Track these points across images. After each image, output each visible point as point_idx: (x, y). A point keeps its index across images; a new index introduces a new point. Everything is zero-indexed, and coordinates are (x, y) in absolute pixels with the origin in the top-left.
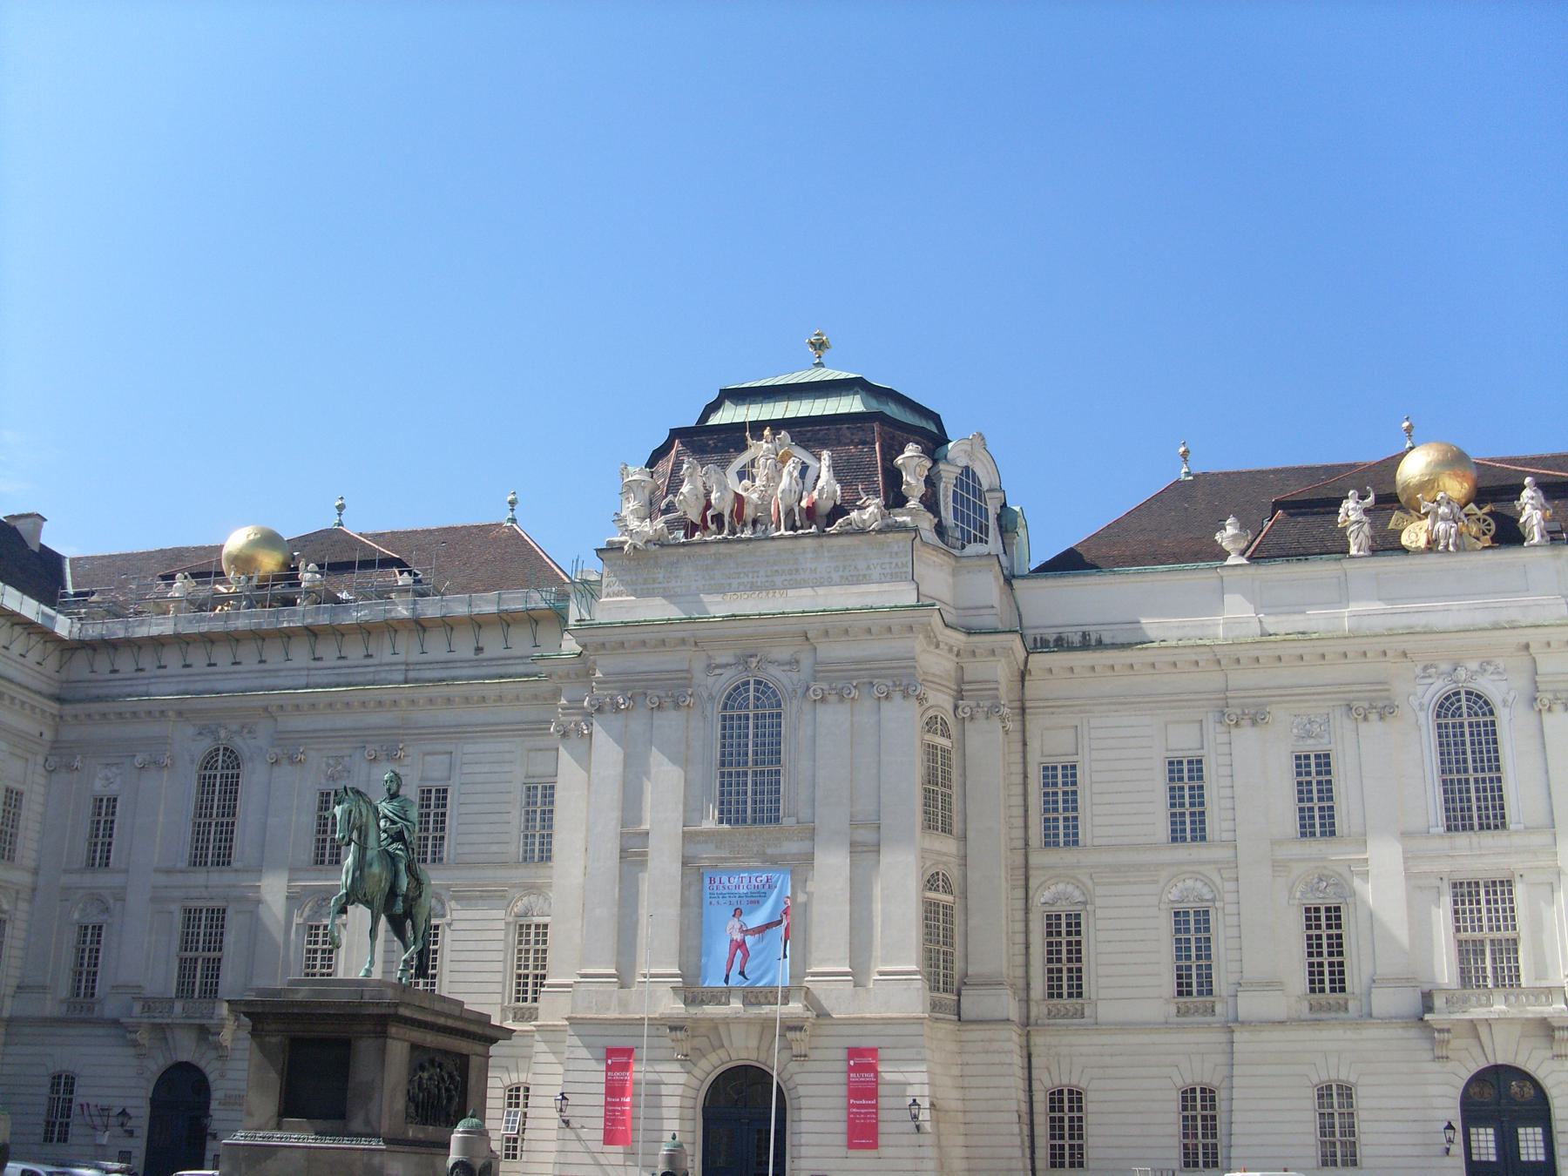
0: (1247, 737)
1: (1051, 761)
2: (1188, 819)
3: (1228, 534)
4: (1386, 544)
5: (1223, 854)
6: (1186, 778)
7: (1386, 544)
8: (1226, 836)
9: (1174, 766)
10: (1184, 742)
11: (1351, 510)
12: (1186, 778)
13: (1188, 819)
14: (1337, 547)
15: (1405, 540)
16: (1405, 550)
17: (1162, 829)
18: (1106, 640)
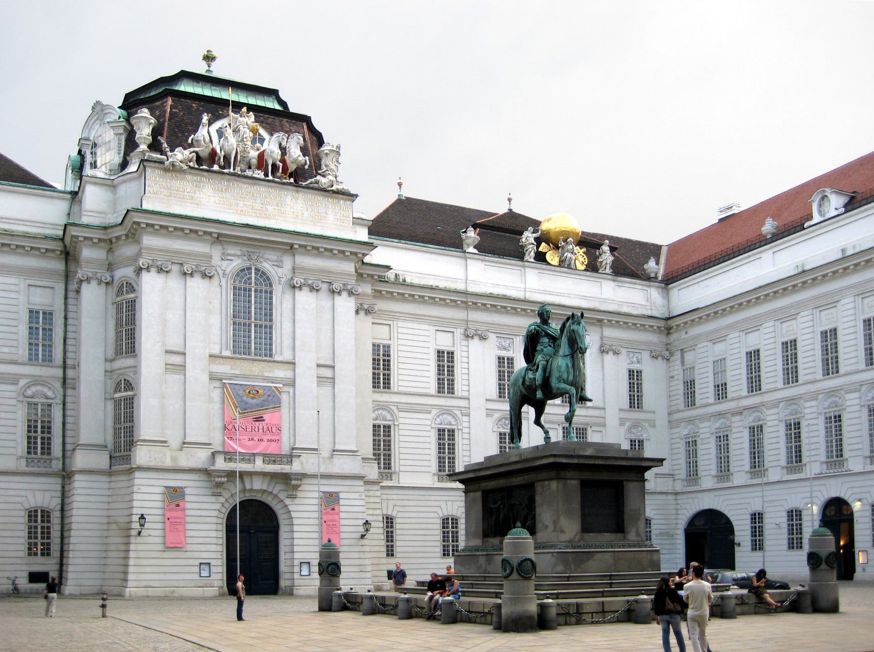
0: (475, 343)
1: (377, 341)
2: (446, 382)
3: (472, 235)
4: (540, 257)
5: (463, 403)
6: (445, 362)
7: (540, 257)
8: (465, 394)
9: (440, 353)
10: (445, 342)
11: (528, 237)
12: (445, 362)
13: (446, 382)
14: (518, 254)
15: (548, 257)
16: (549, 264)
17: (433, 387)
18: (408, 280)
